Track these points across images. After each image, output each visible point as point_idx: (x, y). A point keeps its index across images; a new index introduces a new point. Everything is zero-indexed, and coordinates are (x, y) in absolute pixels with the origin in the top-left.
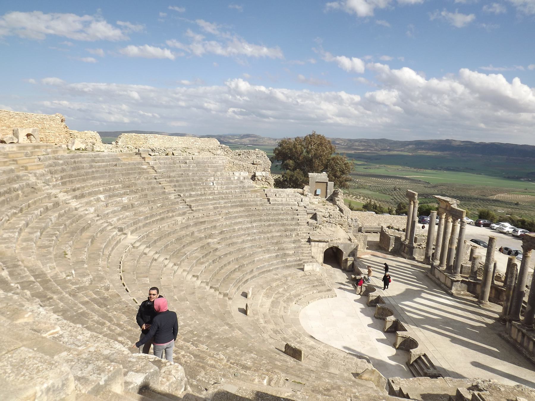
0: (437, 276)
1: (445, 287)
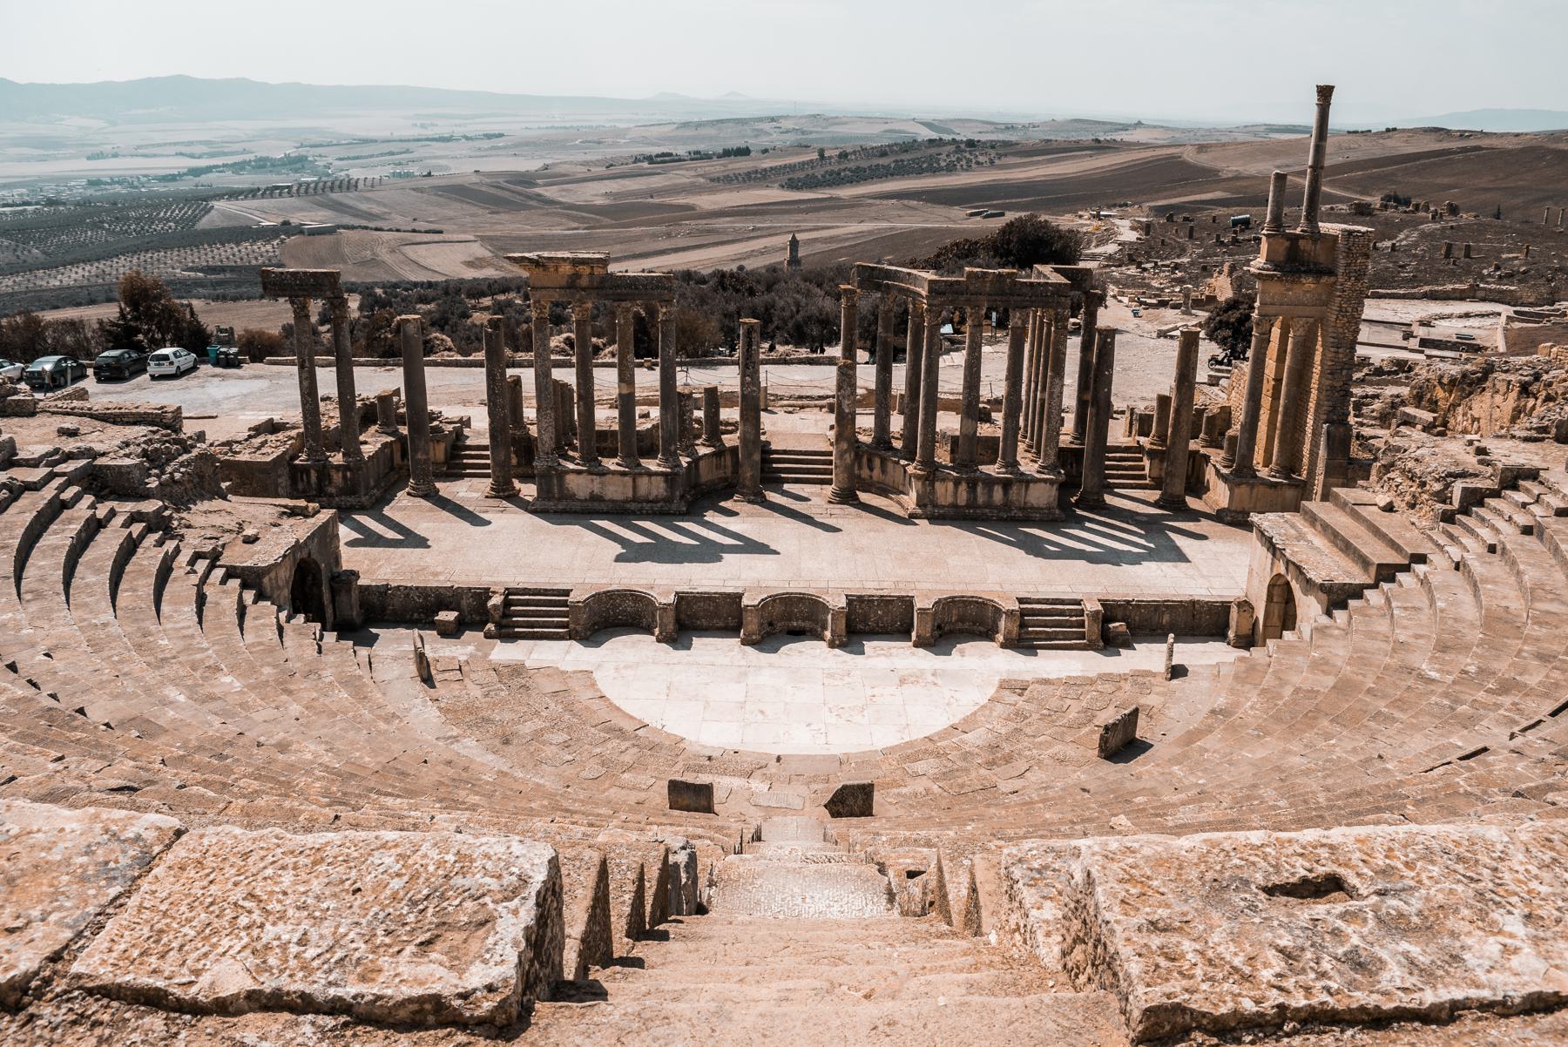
0: (582, 493)
1: (647, 506)
